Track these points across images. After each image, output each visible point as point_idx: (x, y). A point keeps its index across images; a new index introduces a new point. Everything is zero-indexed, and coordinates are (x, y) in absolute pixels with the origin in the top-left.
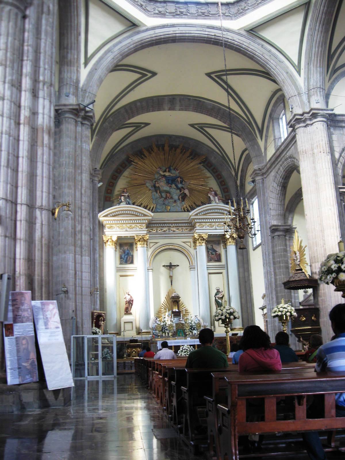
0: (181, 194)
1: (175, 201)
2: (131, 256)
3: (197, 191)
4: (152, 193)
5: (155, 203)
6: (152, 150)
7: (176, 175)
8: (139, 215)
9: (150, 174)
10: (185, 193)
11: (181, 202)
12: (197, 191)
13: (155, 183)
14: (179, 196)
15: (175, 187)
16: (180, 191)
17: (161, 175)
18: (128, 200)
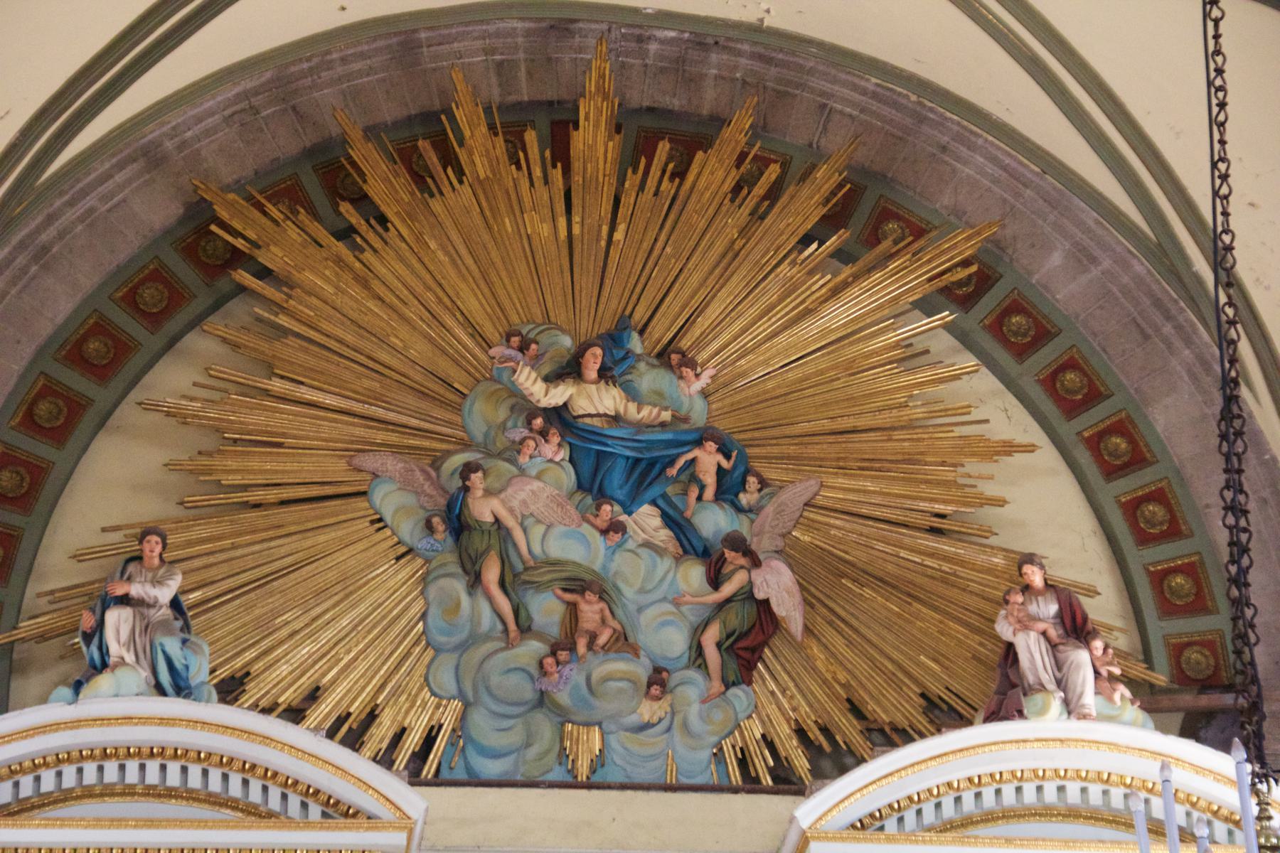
0: (722, 606)
1: (658, 680)
3: (883, 582)
4: (424, 580)
5: (452, 688)
6: (449, 159)
7: (678, 419)
8: (274, 803)
9: (423, 395)
10: (760, 595)
11: (717, 686)
12: (883, 582)
13: (466, 489)
14: (698, 631)
15: (664, 536)
16: (715, 581)
18: (172, 645)
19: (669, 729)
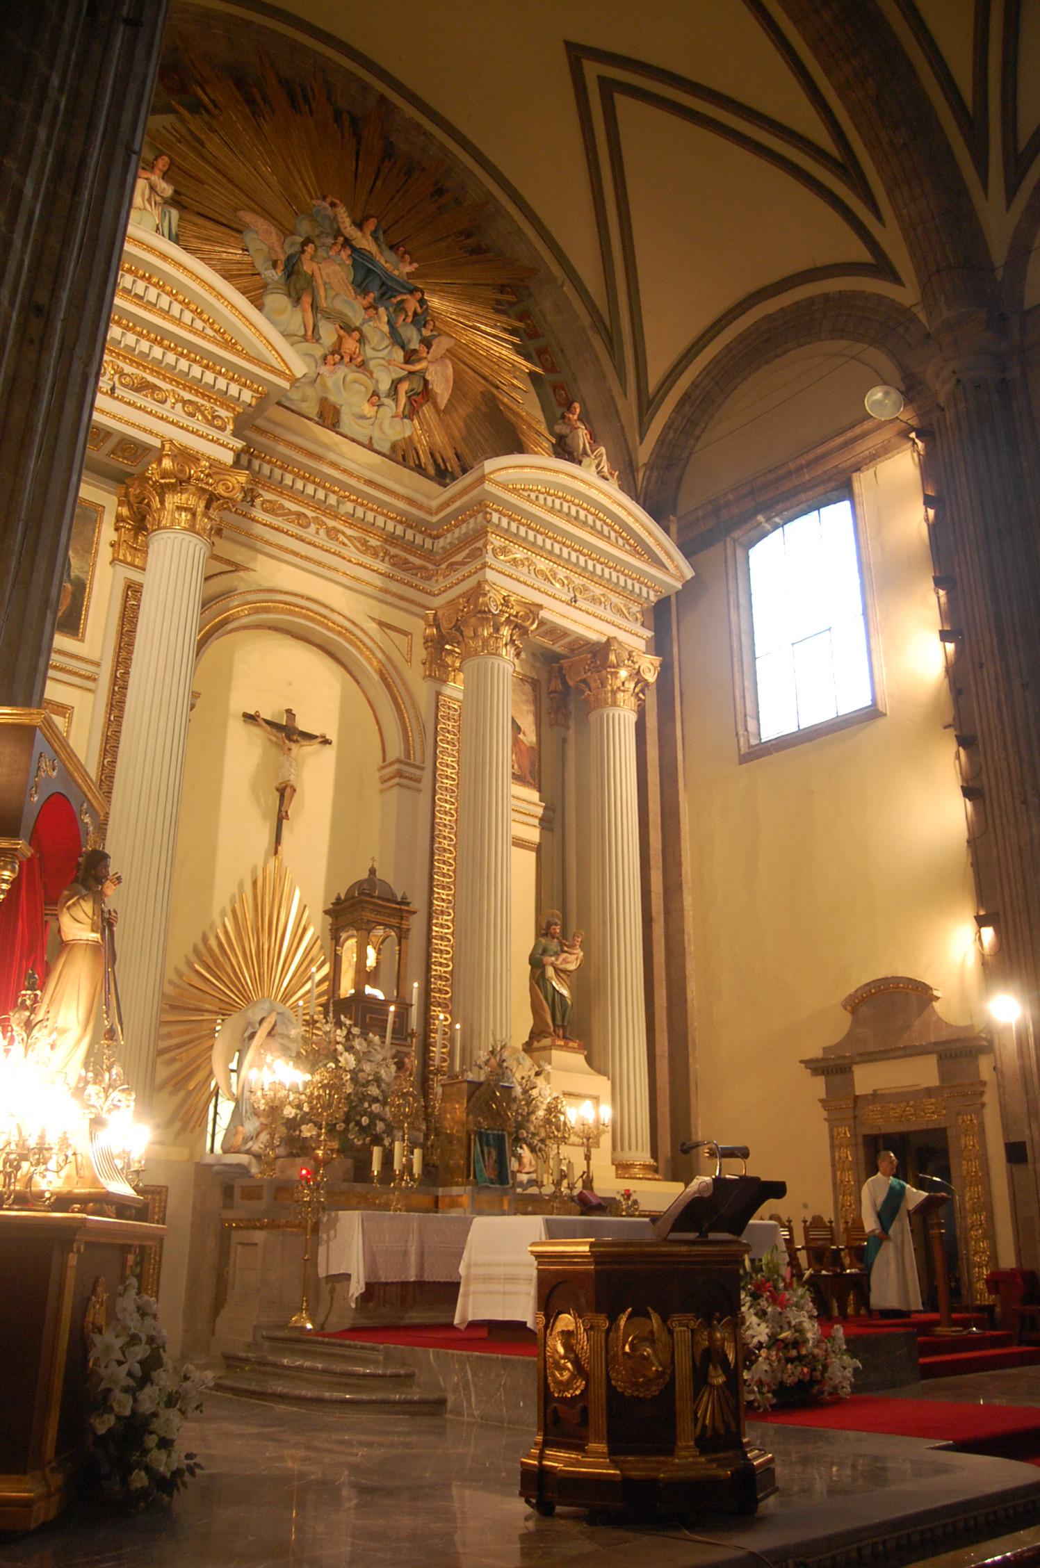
2: (68, 585)
10: (429, 378)
16: (407, 361)
17: (338, 233)
19: (373, 425)
